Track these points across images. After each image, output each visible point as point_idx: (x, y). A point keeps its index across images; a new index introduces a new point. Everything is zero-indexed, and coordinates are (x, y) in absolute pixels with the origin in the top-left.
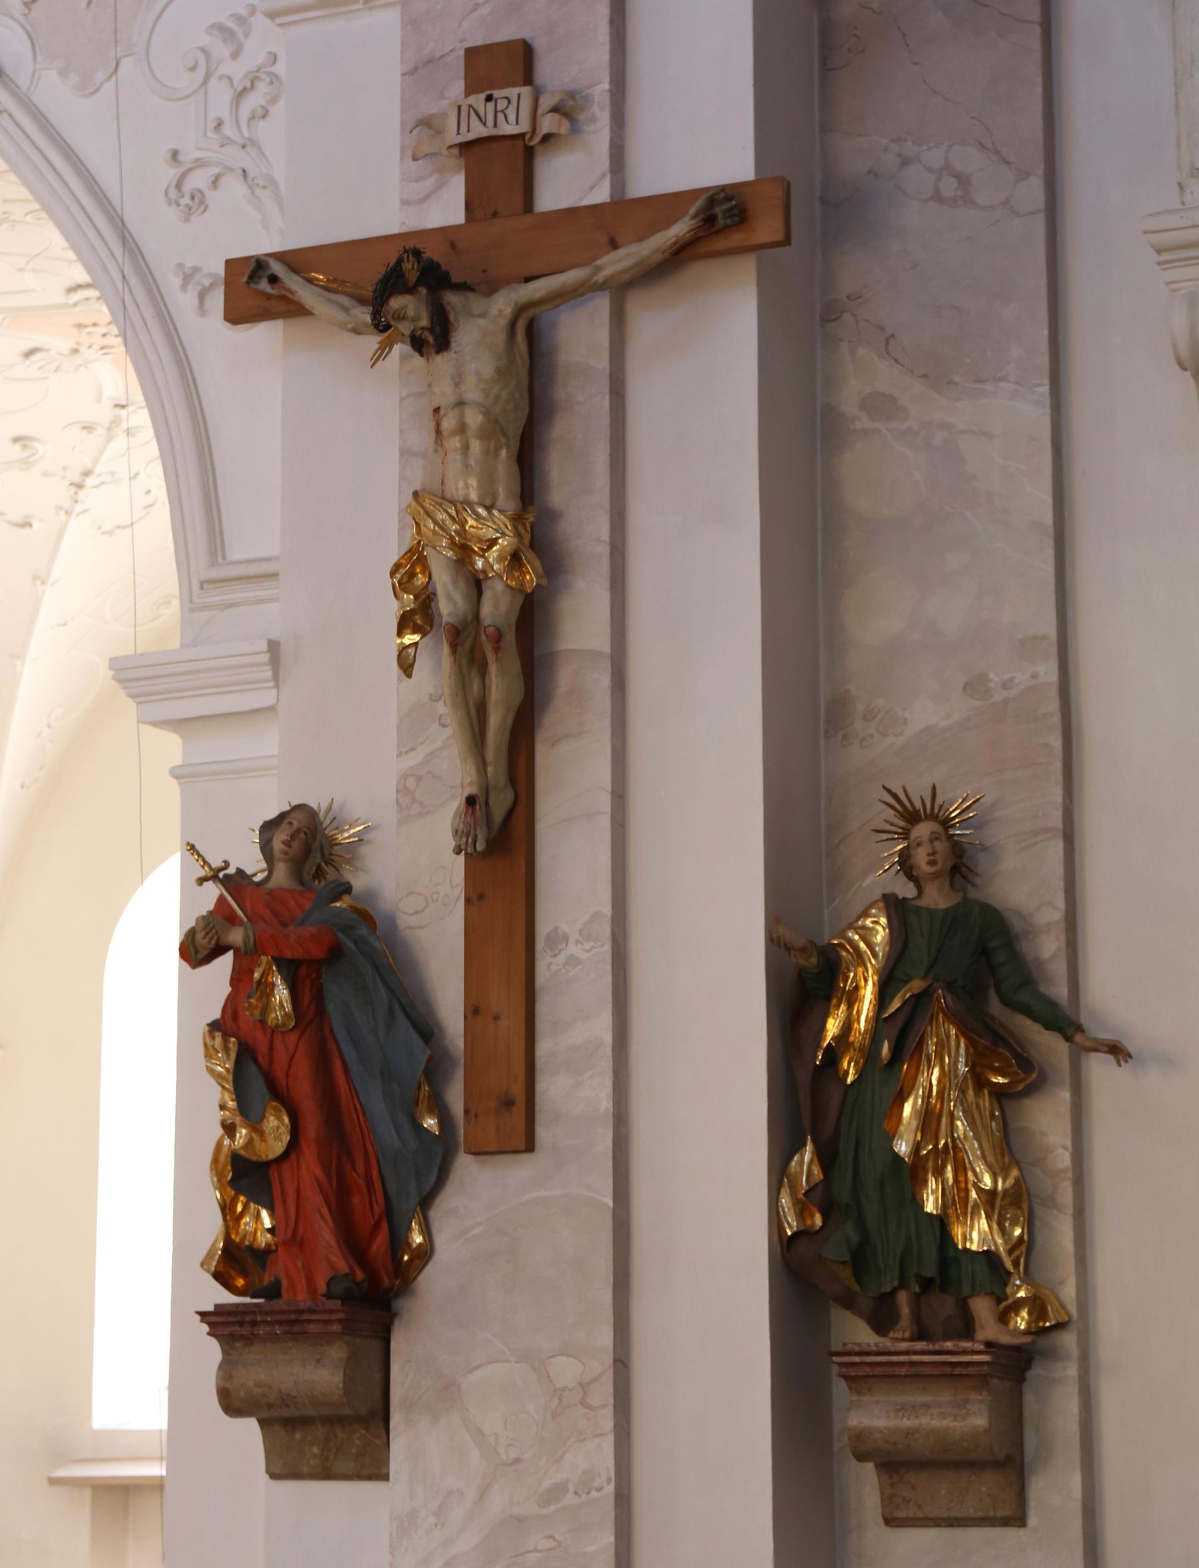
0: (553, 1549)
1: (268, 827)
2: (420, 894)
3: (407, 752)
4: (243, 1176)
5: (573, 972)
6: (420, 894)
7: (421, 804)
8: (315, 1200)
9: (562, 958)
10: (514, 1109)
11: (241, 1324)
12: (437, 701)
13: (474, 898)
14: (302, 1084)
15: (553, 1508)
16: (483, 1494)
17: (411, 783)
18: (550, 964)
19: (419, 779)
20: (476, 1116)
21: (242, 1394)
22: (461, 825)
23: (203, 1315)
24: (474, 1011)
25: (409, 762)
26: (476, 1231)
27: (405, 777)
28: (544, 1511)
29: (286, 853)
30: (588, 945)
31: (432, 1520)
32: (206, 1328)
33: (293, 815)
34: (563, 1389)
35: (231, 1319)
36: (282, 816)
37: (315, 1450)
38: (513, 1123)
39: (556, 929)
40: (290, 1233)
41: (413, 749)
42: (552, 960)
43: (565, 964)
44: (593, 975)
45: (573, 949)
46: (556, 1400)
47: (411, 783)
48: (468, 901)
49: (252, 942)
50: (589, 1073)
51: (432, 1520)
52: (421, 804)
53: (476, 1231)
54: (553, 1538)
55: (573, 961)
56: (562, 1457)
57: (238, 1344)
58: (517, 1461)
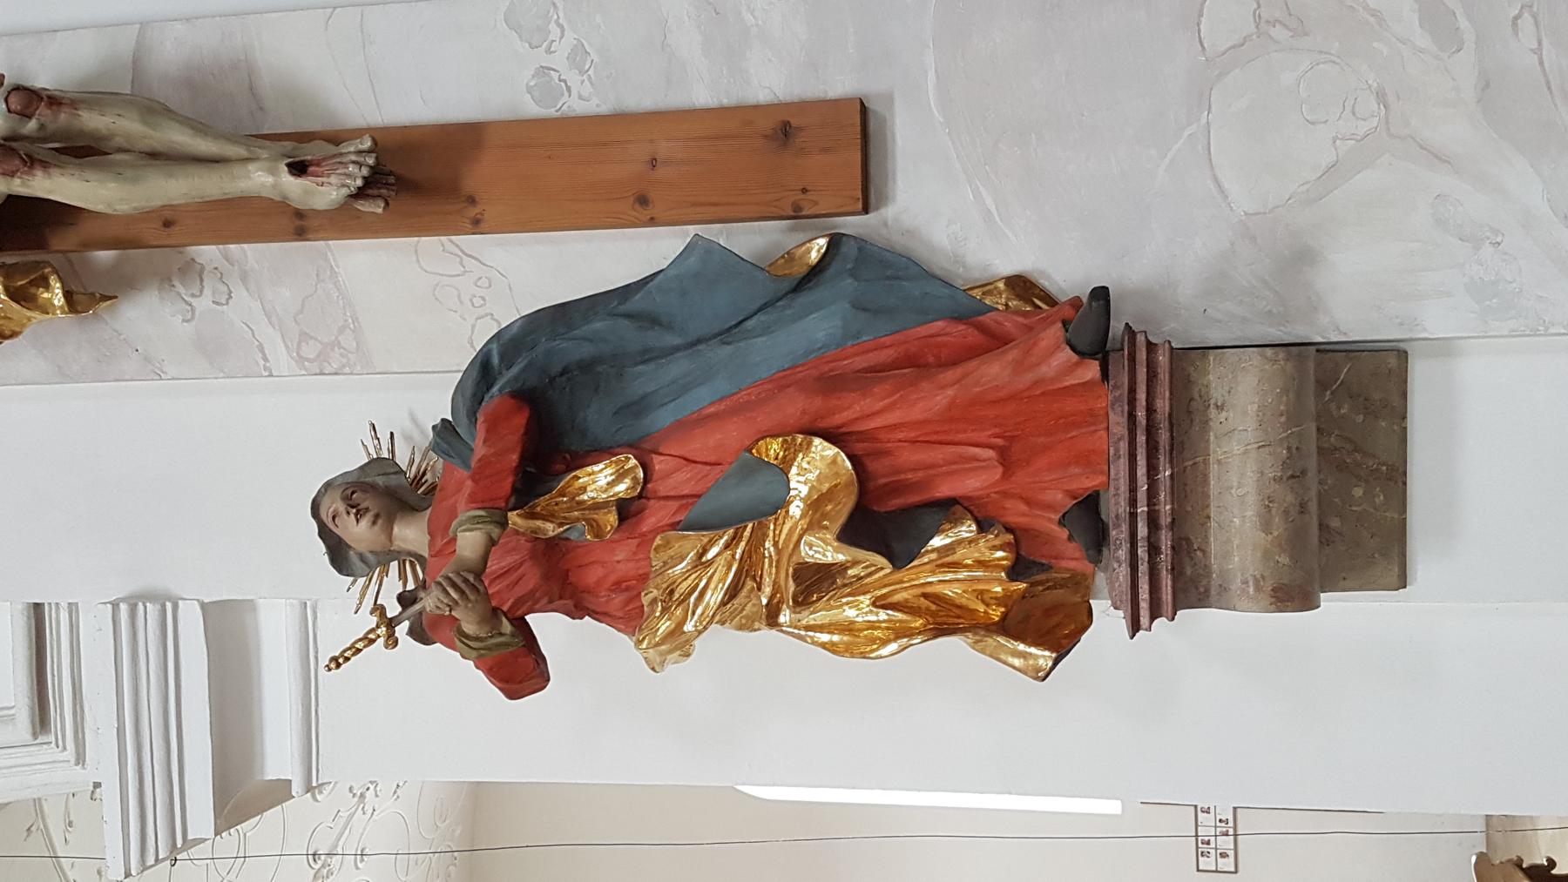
0: (1535, 17)
1: (339, 554)
2: (473, 326)
3: (266, 359)
4: (883, 520)
5: (594, 56)
6: (473, 326)
7: (341, 331)
8: (933, 399)
9: (573, 78)
10: (794, 122)
11: (1154, 550)
12: (193, 310)
13: (473, 212)
14: (731, 434)
15: (1463, 23)
16: (1439, 158)
17: (310, 350)
18: (580, 97)
19: (304, 336)
20: (804, 191)
21: (1284, 559)
22: (333, 179)
23: (1135, 627)
24: (641, 207)
25: (280, 357)
26: (989, 201)
27: (301, 359)
28: (1469, 38)
29: (377, 516)
30: (555, 31)
31: (1487, 251)
32: (1160, 622)
33: (323, 516)
34: (1258, 19)
35: (1143, 568)
36: (325, 533)
37: (1358, 492)
38: (824, 149)
39: (529, 90)
40: (990, 453)
41: (261, 348)
42: (574, 92)
43: (582, 73)
44: (598, 19)
45: (559, 60)
46: (1277, 32)
47: (310, 350)
48: (477, 226)
49: (481, 513)
50: (748, 17)
51: (1487, 251)
52: (341, 331)
53: (989, 201)
54: (1516, 18)
55: (578, 55)
56: (1374, 13)
57: (1189, 571)
58: (1381, 96)
